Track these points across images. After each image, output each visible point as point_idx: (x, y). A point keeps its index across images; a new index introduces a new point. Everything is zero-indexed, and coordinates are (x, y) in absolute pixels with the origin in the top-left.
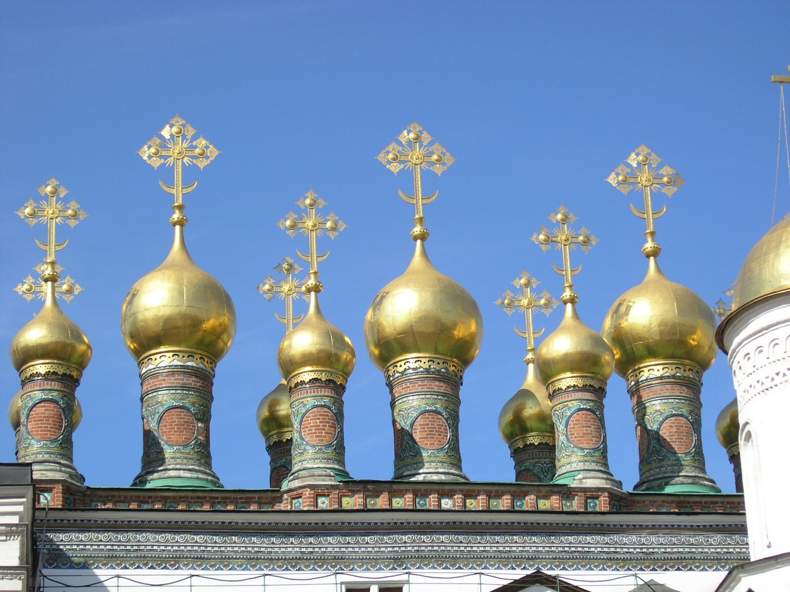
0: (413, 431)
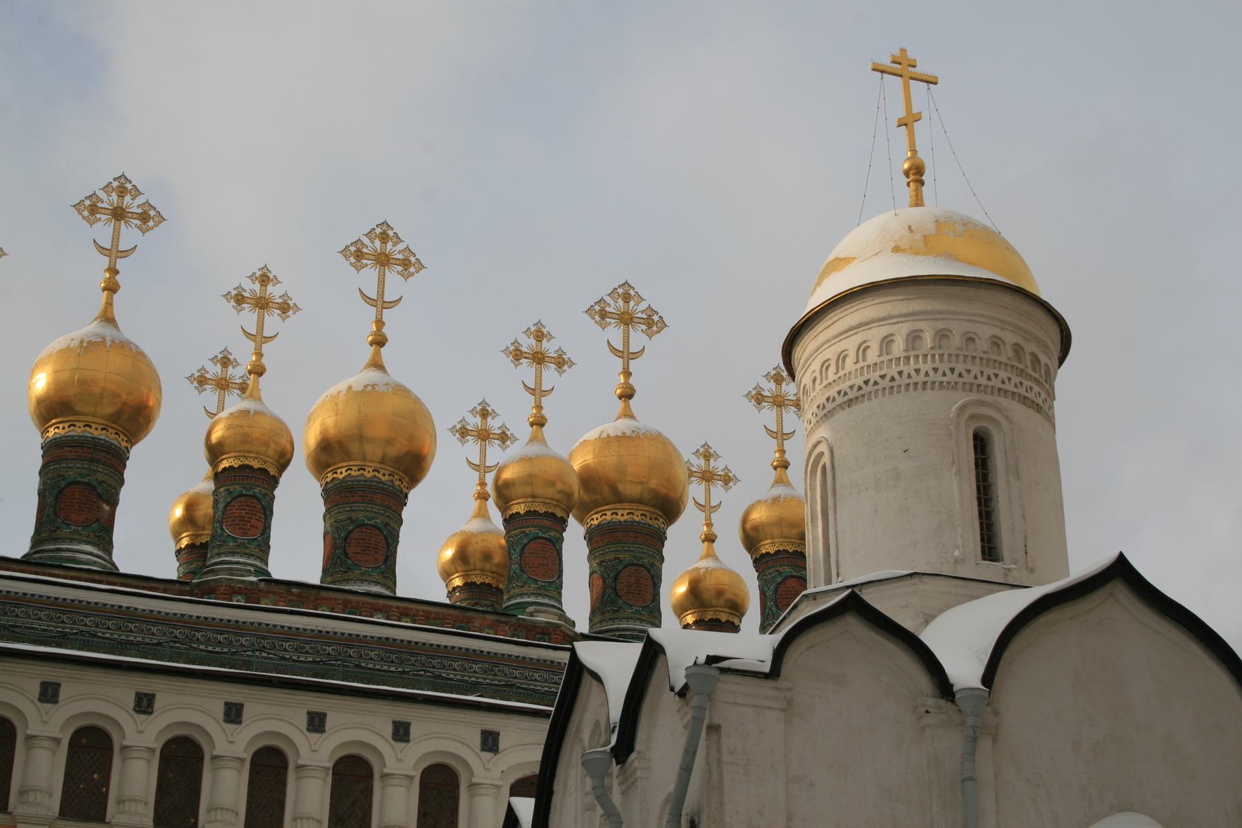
0: (347, 545)
